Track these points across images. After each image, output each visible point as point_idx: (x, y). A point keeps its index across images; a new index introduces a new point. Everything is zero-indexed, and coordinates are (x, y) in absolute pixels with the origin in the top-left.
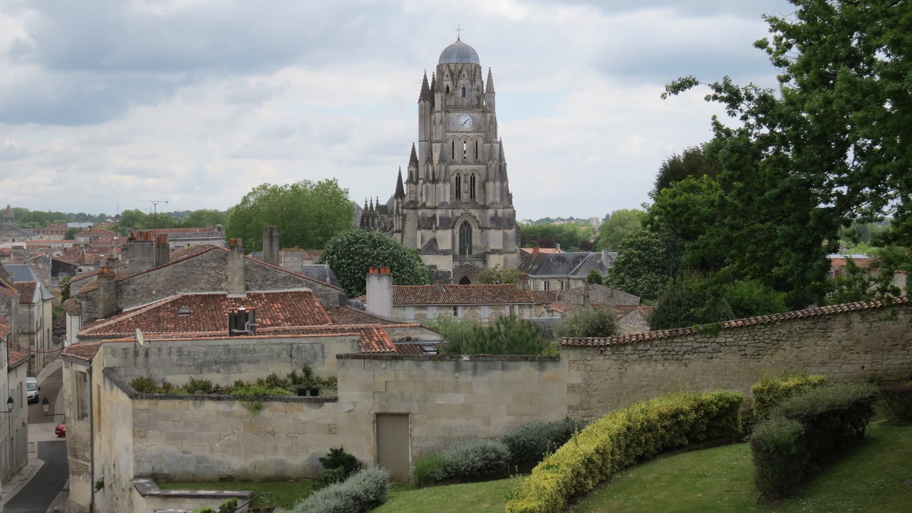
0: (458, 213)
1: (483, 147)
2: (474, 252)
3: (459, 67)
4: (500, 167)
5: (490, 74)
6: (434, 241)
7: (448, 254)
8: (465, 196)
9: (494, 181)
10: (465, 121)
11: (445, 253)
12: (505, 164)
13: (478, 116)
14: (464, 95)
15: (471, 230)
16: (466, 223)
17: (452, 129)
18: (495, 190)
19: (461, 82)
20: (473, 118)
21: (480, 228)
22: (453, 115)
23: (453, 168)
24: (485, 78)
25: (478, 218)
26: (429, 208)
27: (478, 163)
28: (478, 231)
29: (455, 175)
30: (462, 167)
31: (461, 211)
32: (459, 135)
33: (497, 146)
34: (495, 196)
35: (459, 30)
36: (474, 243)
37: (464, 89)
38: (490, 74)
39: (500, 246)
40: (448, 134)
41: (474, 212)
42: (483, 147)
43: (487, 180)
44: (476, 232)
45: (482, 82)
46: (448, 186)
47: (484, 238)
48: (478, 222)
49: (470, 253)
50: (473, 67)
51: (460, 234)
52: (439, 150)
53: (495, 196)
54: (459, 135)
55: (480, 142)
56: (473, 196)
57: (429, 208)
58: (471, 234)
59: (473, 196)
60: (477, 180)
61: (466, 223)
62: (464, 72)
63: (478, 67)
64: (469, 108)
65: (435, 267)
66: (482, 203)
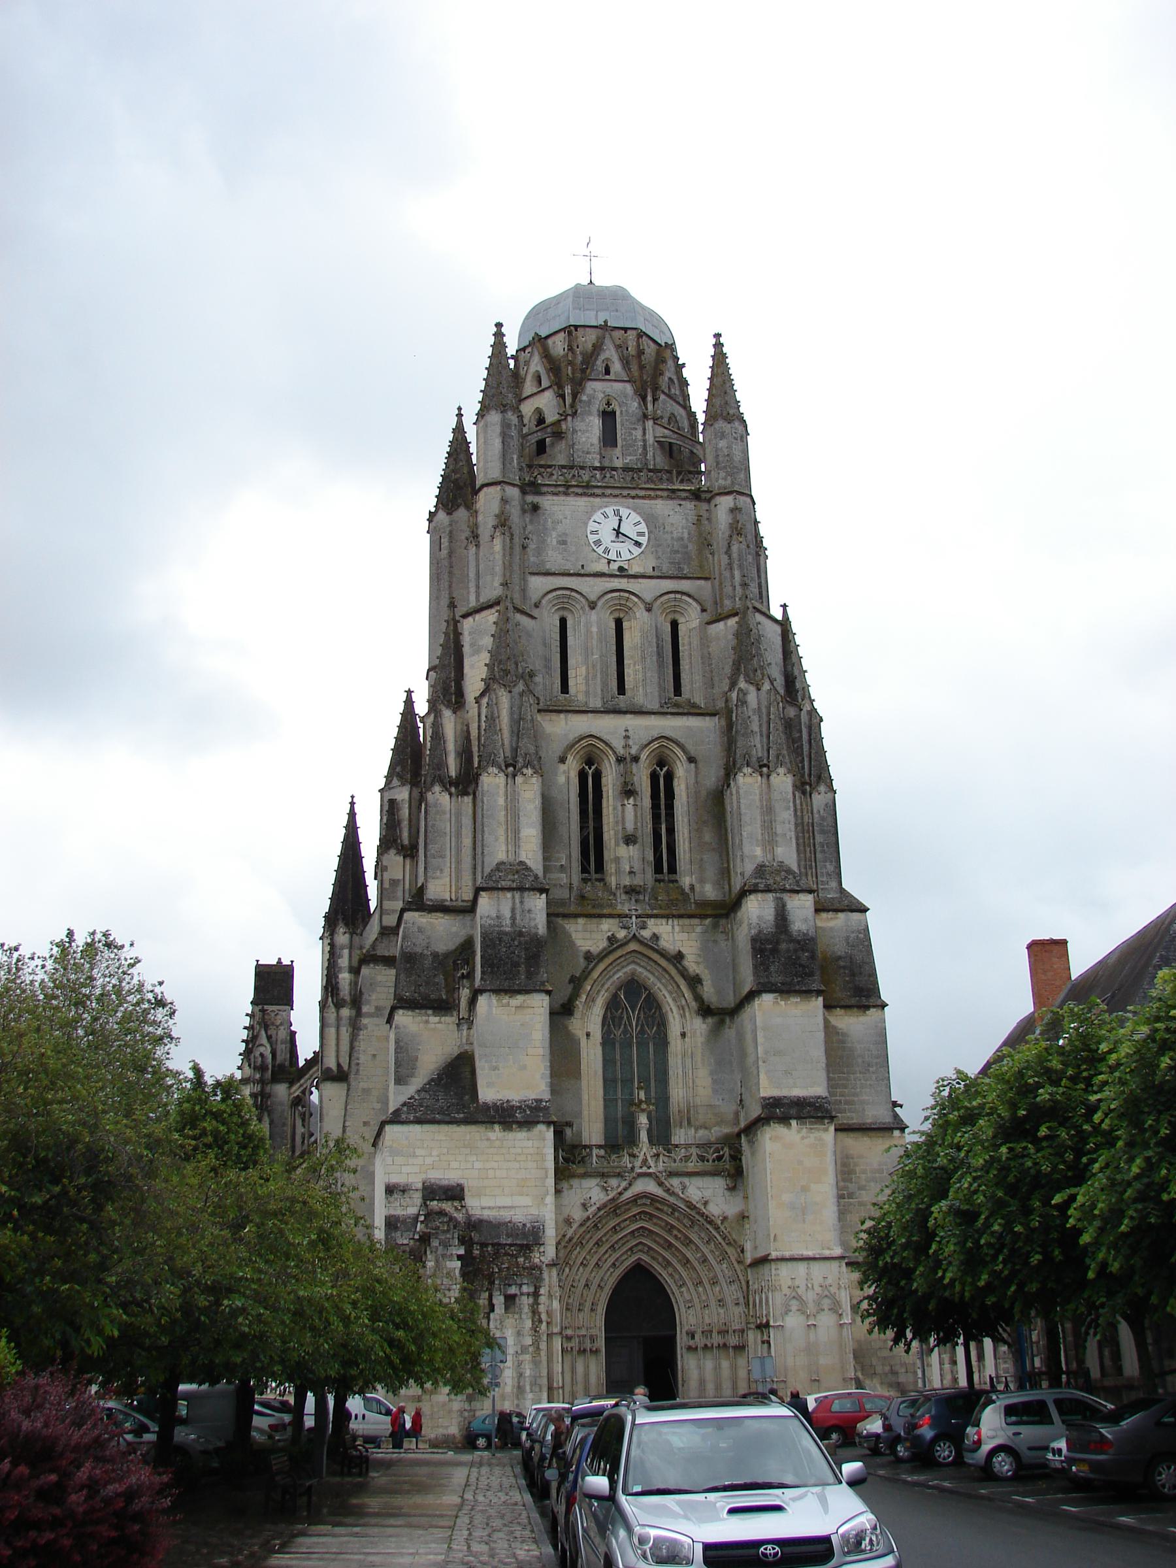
0: (589, 937)
1: (705, 641)
2: (680, 1136)
3: (587, 340)
4: (790, 726)
5: (719, 360)
6: (458, 1075)
7: (528, 1124)
8: (626, 860)
9: (763, 767)
10: (612, 532)
11: (506, 1117)
12: (815, 720)
13: (677, 515)
14: (609, 437)
15: (662, 1024)
16: (633, 987)
17: (554, 559)
18: (768, 810)
19: (596, 390)
20: (651, 520)
21: (705, 1011)
22: (560, 509)
23: (561, 729)
24: (698, 402)
25: (692, 964)
26: (441, 908)
27: (693, 710)
28: (699, 1026)
29: (572, 766)
30: (609, 727)
31: (608, 926)
32: (592, 588)
33: (773, 633)
34: (770, 841)
35: (590, 257)
36: (677, 1093)
37: (608, 417)
38: (719, 360)
39: (812, 1086)
40: (538, 585)
41: (673, 935)
42: (707, 641)
43: (730, 771)
44: (685, 1031)
45: (692, 416)
46: (529, 791)
47: (733, 1062)
48: (695, 982)
49: (661, 1136)
50: (650, 349)
51: (607, 1042)
52: (487, 641)
53: (770, 841)
54: (592, 588)
55: (691, 620)
56: (664, 861)
57: (441, 908)
58: (662, 1042)
59: (664, 861)
60: (680, 788)
61: (633, 987)
62: (610, 352)
63: (666, 352)
64: (631, 483)
65: (455, 1193)
66: (709, 892)
